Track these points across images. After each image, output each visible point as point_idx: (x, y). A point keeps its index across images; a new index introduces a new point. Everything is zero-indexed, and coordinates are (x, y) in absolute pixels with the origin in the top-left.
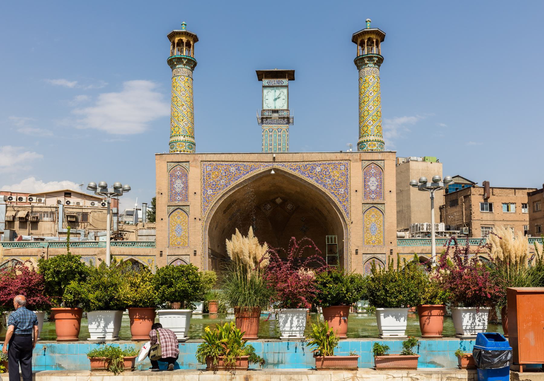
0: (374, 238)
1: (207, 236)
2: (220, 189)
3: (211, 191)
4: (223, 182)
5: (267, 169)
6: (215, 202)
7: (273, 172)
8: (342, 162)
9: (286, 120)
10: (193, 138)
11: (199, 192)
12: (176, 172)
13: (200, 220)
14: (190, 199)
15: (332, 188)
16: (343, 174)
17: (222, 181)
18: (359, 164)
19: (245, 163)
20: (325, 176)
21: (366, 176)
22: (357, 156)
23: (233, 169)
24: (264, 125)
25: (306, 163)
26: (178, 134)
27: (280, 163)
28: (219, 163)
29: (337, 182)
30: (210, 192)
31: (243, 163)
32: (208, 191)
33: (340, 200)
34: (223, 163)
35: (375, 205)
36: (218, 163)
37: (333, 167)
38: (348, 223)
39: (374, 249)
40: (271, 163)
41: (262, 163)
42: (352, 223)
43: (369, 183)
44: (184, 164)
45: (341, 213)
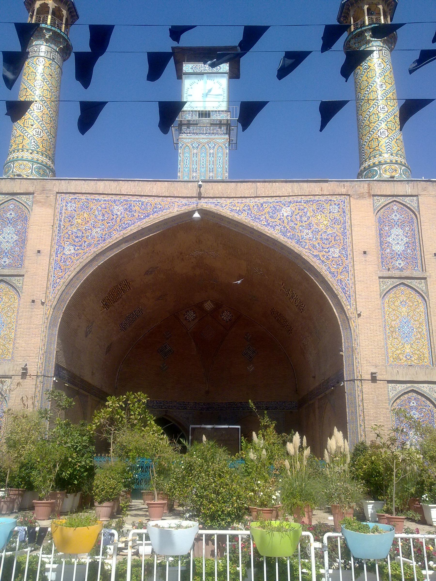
0: (408, 349)
1: (56, 339)
2: (89, 245)
3: (72, 248)
4: (97, 232)
5: (184, 209)
6: (78, 269)
7: (197, 215)
8: (334, 198)
9: (224, 128)
10: (53, 162)
11: (46, 248)
12: (5, 212)
13: (43, 303)
14: (26, 263)
15: (314, 246)
16: (335, 221)
17: (94, 230)
18: (368, 202)
19: (143, 199)
20: (299, 224)
21: (383, 226)
22: (362, 187)
23: (118, 209)
24: (184, 136)
25: (262, 200)
26: (20, 147)
27: (211, 200)
28: (92, 197)
29: (324, 236)
30: (69, 250)
31: (139, 198)
32: (67, 248)
33: (333, 270)
34: (101, 197)
35: (405, 281)
36: (89, 197)
37: (315, 206)
38: (349, 314)
39: (412, 371)
40: (194, 200)
41: (177, 199)
42: (359, 315)
43: (390, 239)
44: (24, 197)
45: (335, 296)
